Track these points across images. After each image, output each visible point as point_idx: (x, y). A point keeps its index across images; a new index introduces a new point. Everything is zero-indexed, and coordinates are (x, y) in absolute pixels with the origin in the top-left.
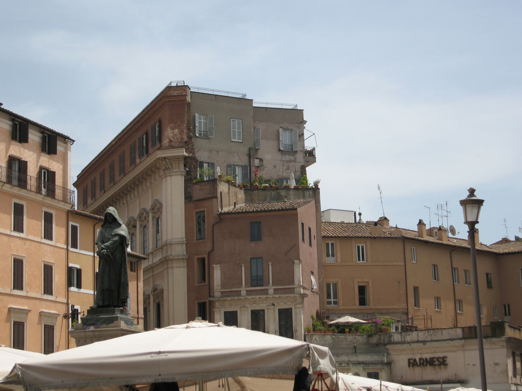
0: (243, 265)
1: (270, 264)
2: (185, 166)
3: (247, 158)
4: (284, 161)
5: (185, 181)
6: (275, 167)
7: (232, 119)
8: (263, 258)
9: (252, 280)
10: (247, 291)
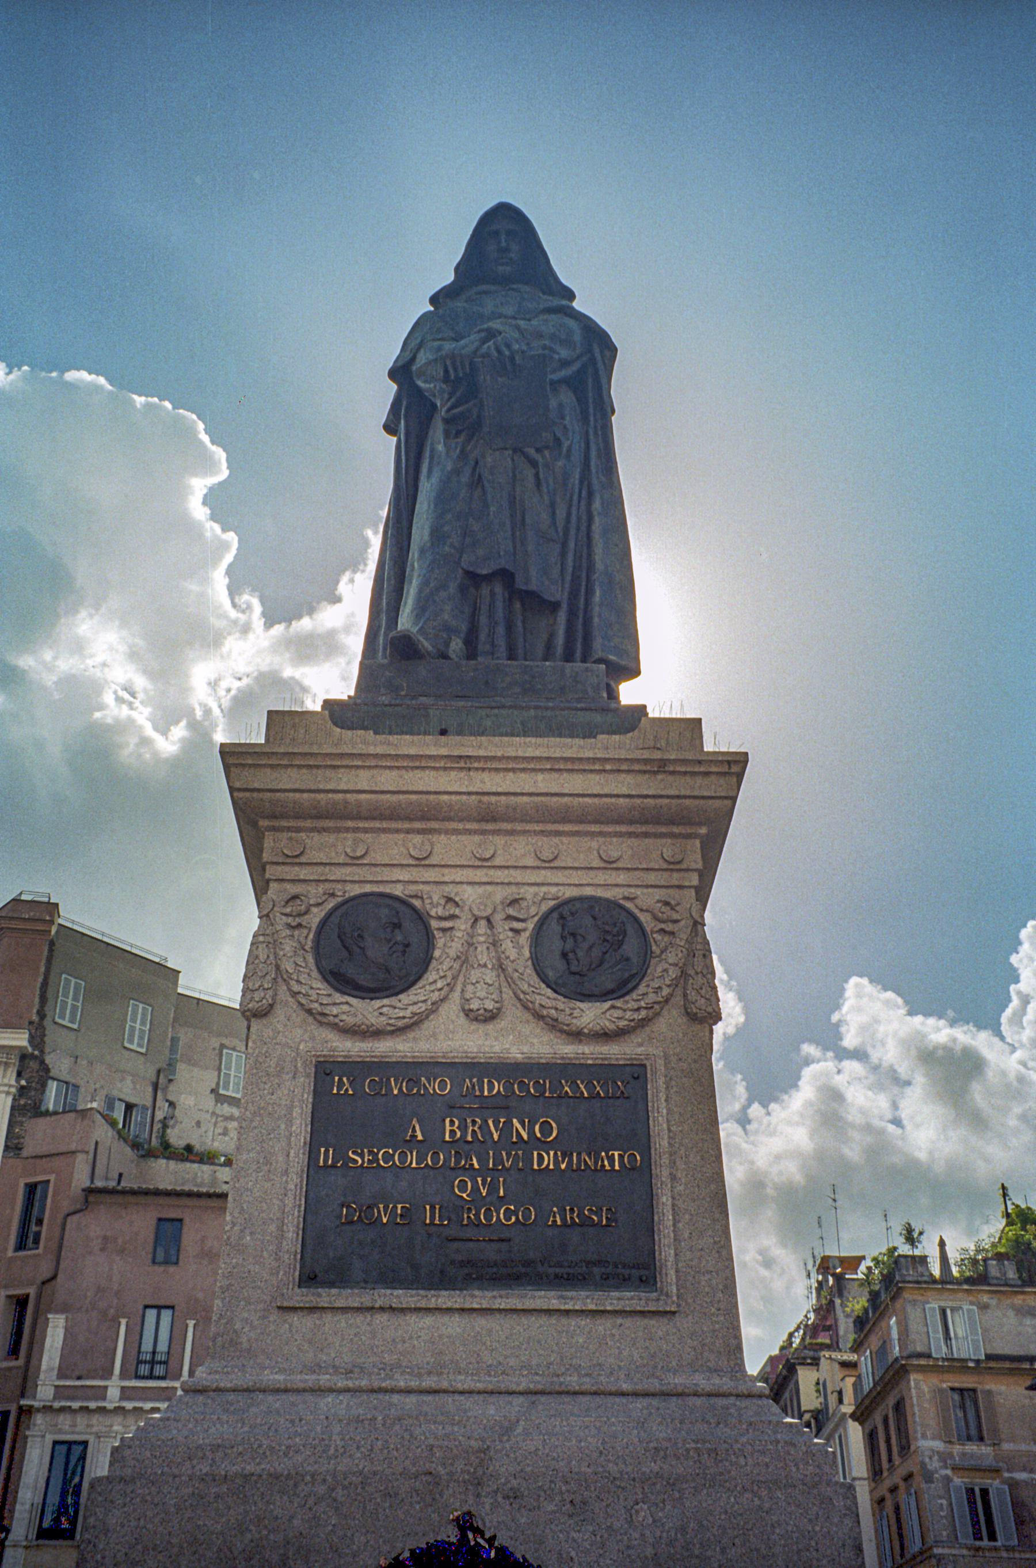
0: (123, 1322)
1: (191, 1323)
2: (19, 1074)
3: (150, 1089)
4: (218, 1116)
5: (13, 1108)
6: (198, 1124)
7: (132, 1002)
8: (176, 1308)
9: (140, 1362)
10: (123, 1389)
